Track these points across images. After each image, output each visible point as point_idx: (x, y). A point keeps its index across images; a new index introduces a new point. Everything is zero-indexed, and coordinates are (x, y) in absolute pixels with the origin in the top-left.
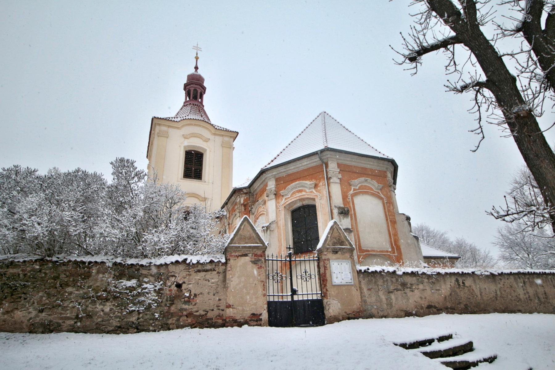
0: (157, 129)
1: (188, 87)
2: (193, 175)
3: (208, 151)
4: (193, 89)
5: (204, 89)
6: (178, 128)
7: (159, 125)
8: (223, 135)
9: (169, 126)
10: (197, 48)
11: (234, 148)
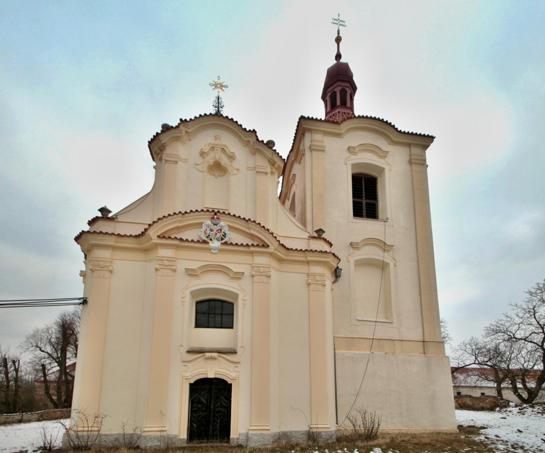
3: (387, 173)
4: (340, 88)
5: (354, 88)
6: (338, 135)
7: (310, 130)
11: (427, 166)
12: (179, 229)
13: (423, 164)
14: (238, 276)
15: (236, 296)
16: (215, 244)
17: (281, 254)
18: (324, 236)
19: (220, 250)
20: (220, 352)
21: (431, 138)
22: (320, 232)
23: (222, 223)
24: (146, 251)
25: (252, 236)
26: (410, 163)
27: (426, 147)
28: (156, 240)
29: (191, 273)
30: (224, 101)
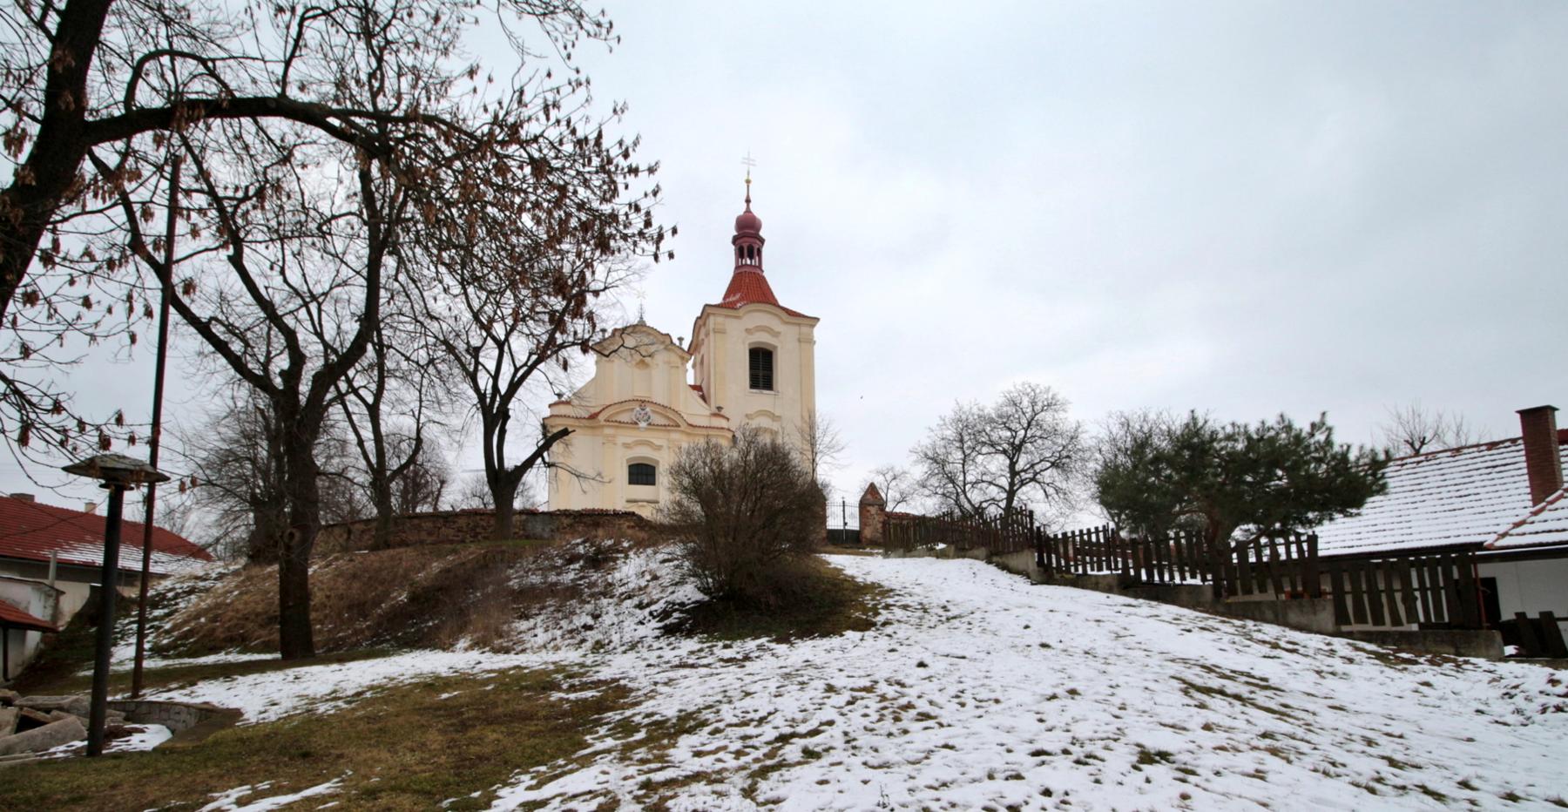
0: (712, 321)
1: (739, 242)
2: (761, 384)
5: (762, 241)
6: (737, 317)
8: (799, 325)
9: (727, 316)
10: (748, 161)
12: (618, 413)
13: (811, 342)
14: (659, 448)
15: (657, 462)
16: (643, 424)
17: (689, 430)
18: (722, 412)
19: (646, 429)
20: (648, 502)
21: (818, 319)
22: (719, 408)
23: (648, 409)
24: (592, 428)
25: (668, 418)
26: (799, 341)
27: (813, 326)
28: (603, 423)
29: (627, 446)
30: (645, 307)
